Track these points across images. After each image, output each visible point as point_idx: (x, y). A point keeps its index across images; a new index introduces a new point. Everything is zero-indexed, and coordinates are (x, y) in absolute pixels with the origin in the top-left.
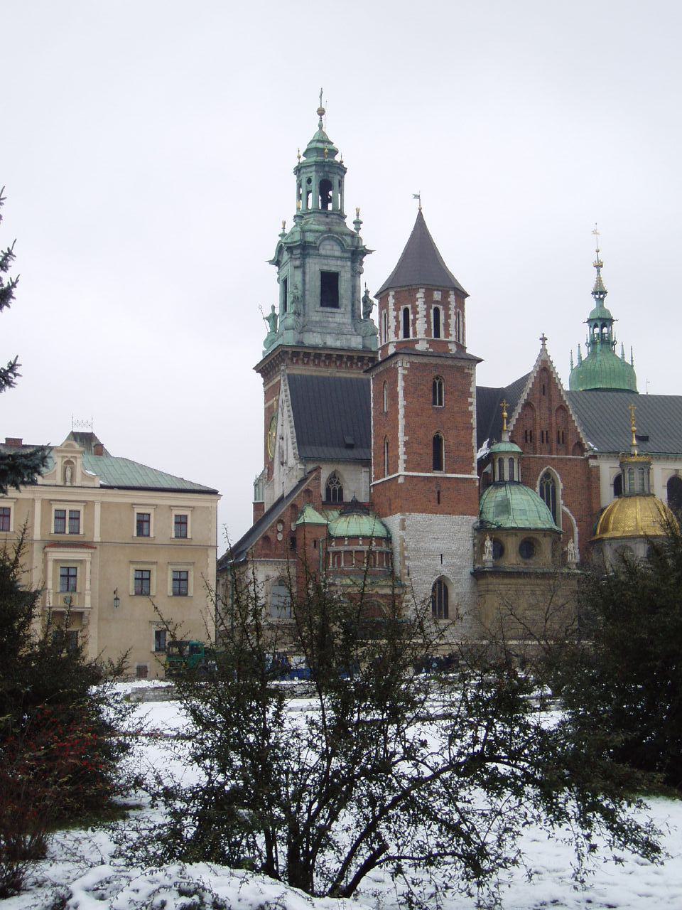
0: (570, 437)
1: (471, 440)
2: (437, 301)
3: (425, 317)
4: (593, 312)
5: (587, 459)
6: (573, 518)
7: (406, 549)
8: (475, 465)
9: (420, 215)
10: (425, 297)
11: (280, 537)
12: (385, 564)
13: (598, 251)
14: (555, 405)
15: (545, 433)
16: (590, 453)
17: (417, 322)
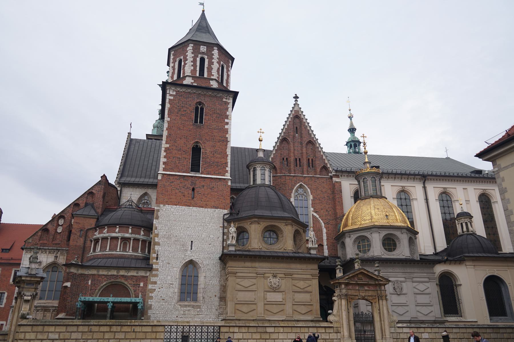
0: (317, 162)
1: (226, 150)
2: (203, 52)
3: (192, 62)
4: (349, 138)
5: (331, 177)
6: (321, 221)
7: (157, 235)
8: (228, 169)
9: (203, 14)
10: (193, 50)
11: (59, 230)
12: (140, 250)
13: (350, 110)
14: (306, 140)
15: (298, 160)
16: (333, 173)
17: (186, 66)
